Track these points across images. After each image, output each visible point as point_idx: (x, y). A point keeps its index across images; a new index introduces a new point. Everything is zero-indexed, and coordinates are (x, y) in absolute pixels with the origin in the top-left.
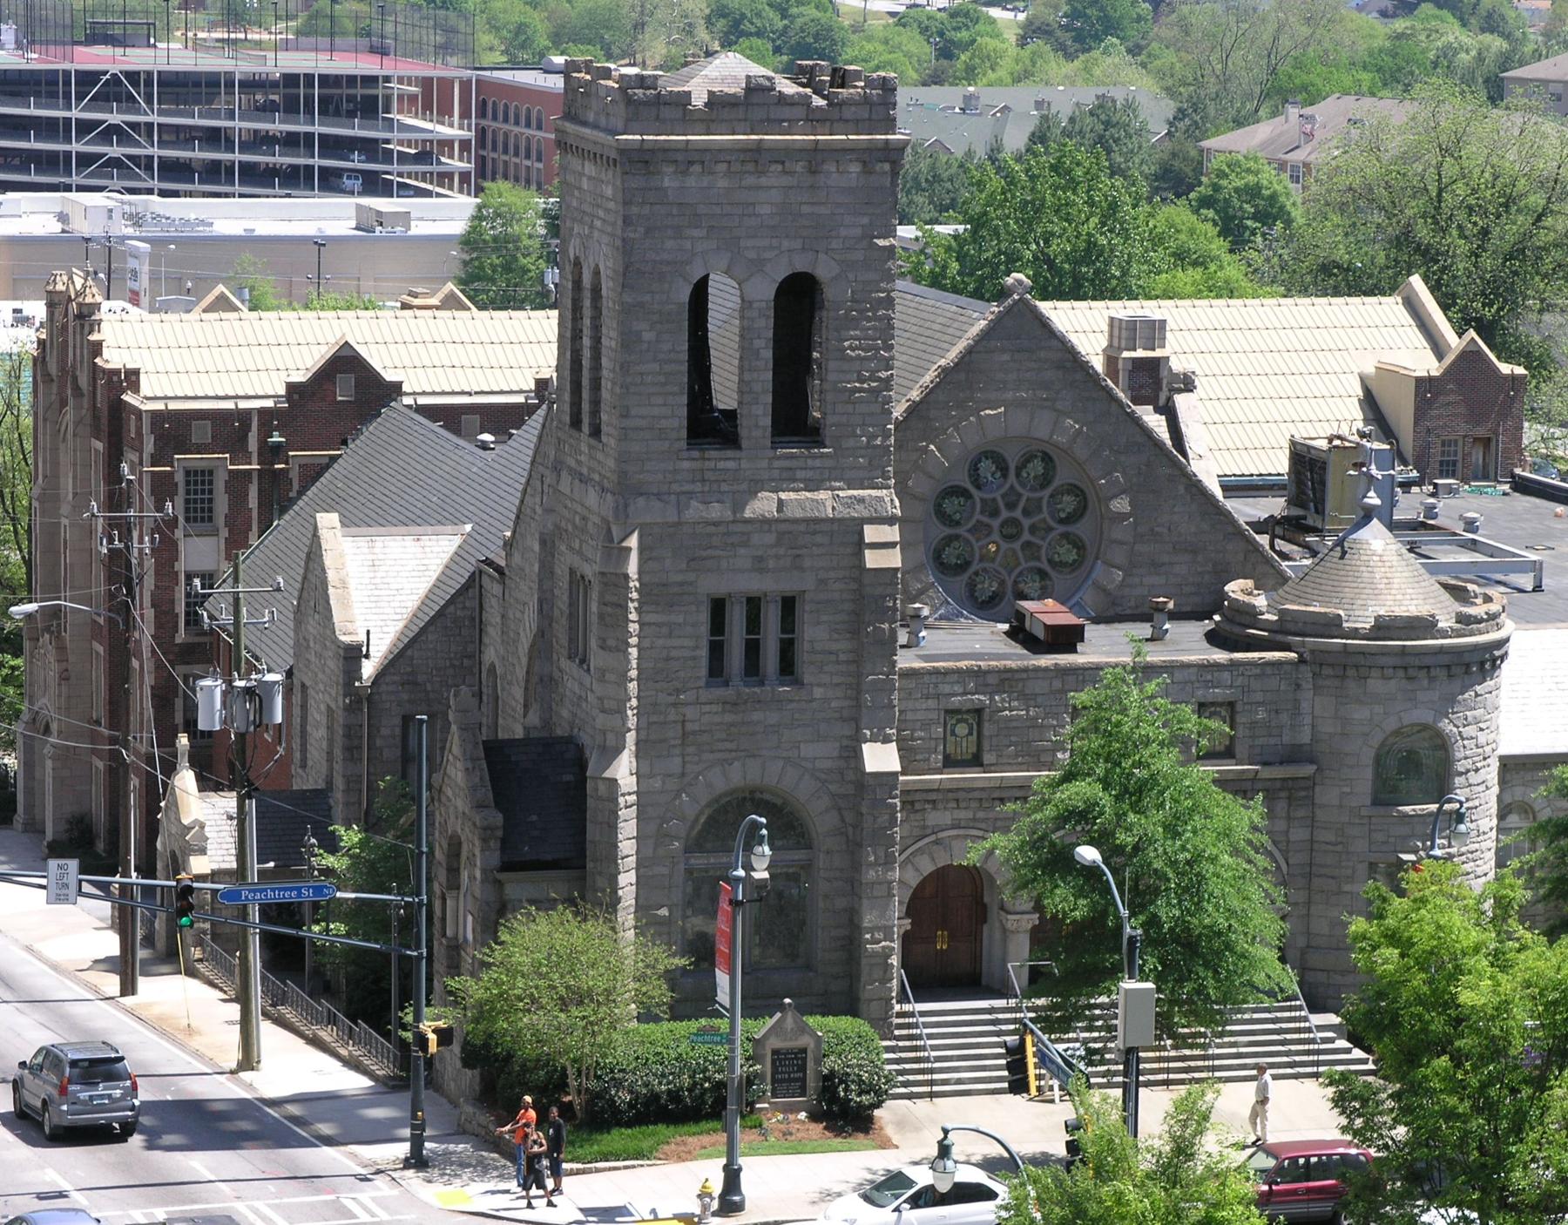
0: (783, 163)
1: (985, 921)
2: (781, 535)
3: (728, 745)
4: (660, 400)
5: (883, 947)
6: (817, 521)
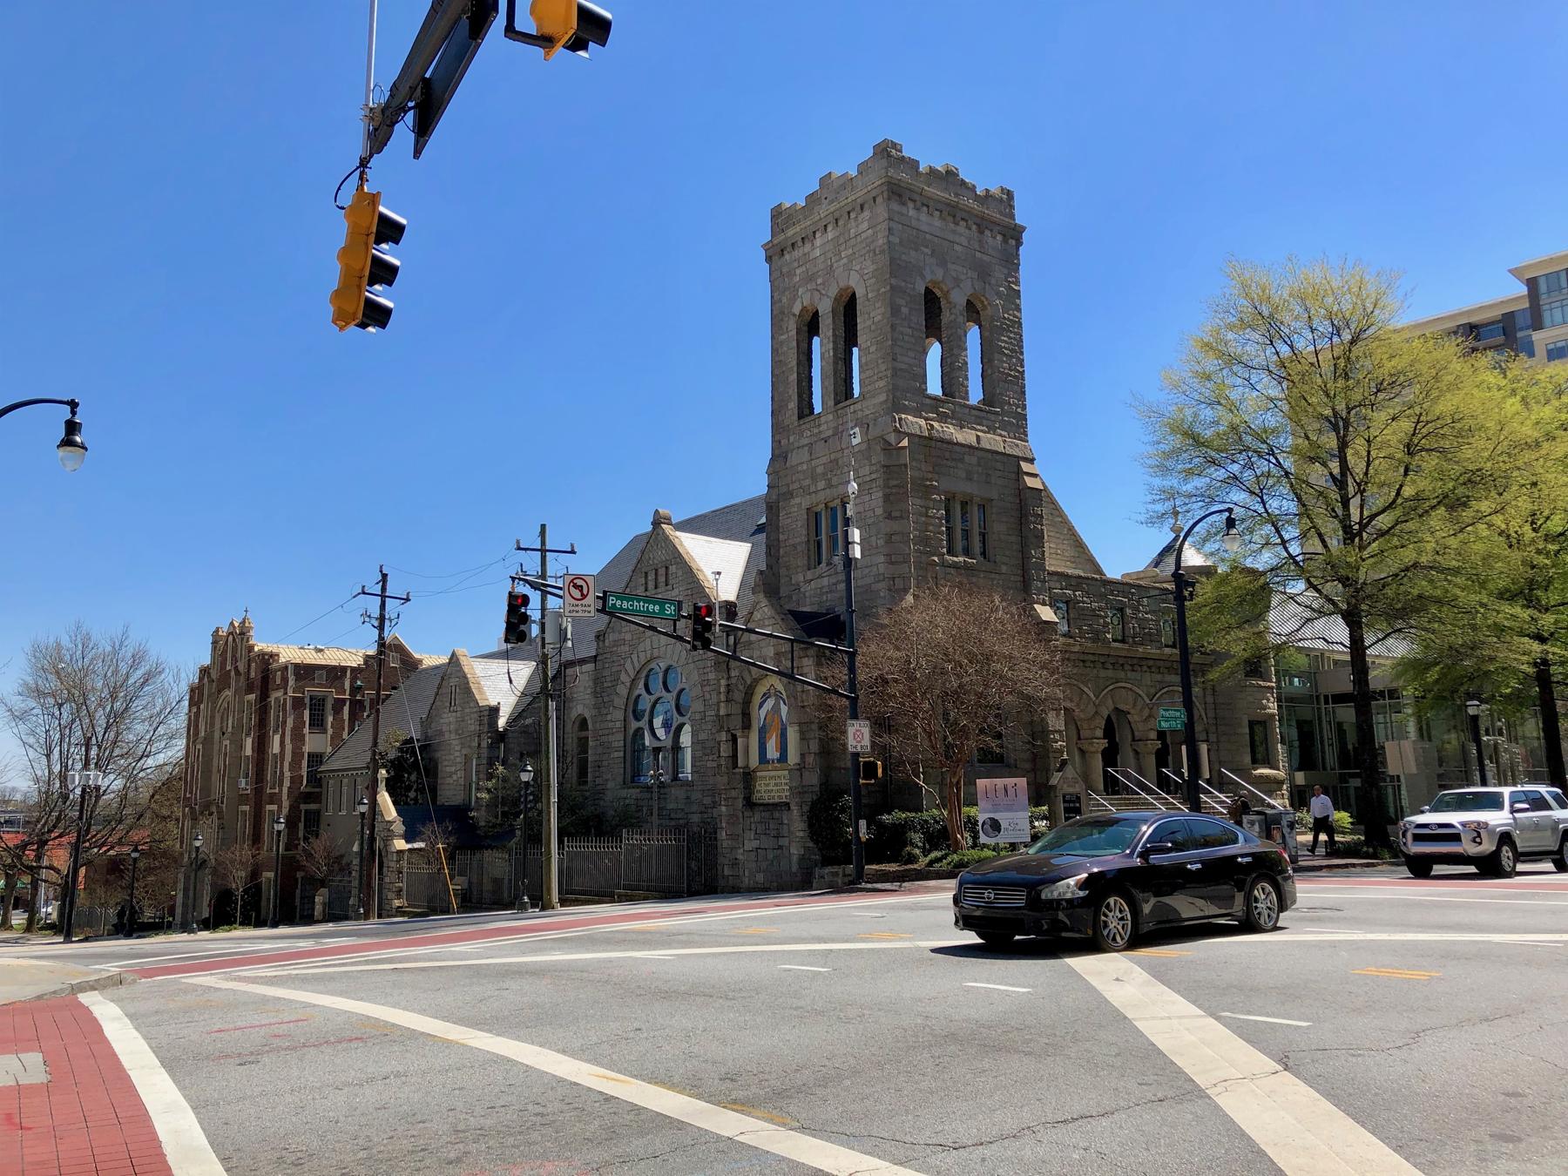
0: (967, 221)
5: (1061, 745)
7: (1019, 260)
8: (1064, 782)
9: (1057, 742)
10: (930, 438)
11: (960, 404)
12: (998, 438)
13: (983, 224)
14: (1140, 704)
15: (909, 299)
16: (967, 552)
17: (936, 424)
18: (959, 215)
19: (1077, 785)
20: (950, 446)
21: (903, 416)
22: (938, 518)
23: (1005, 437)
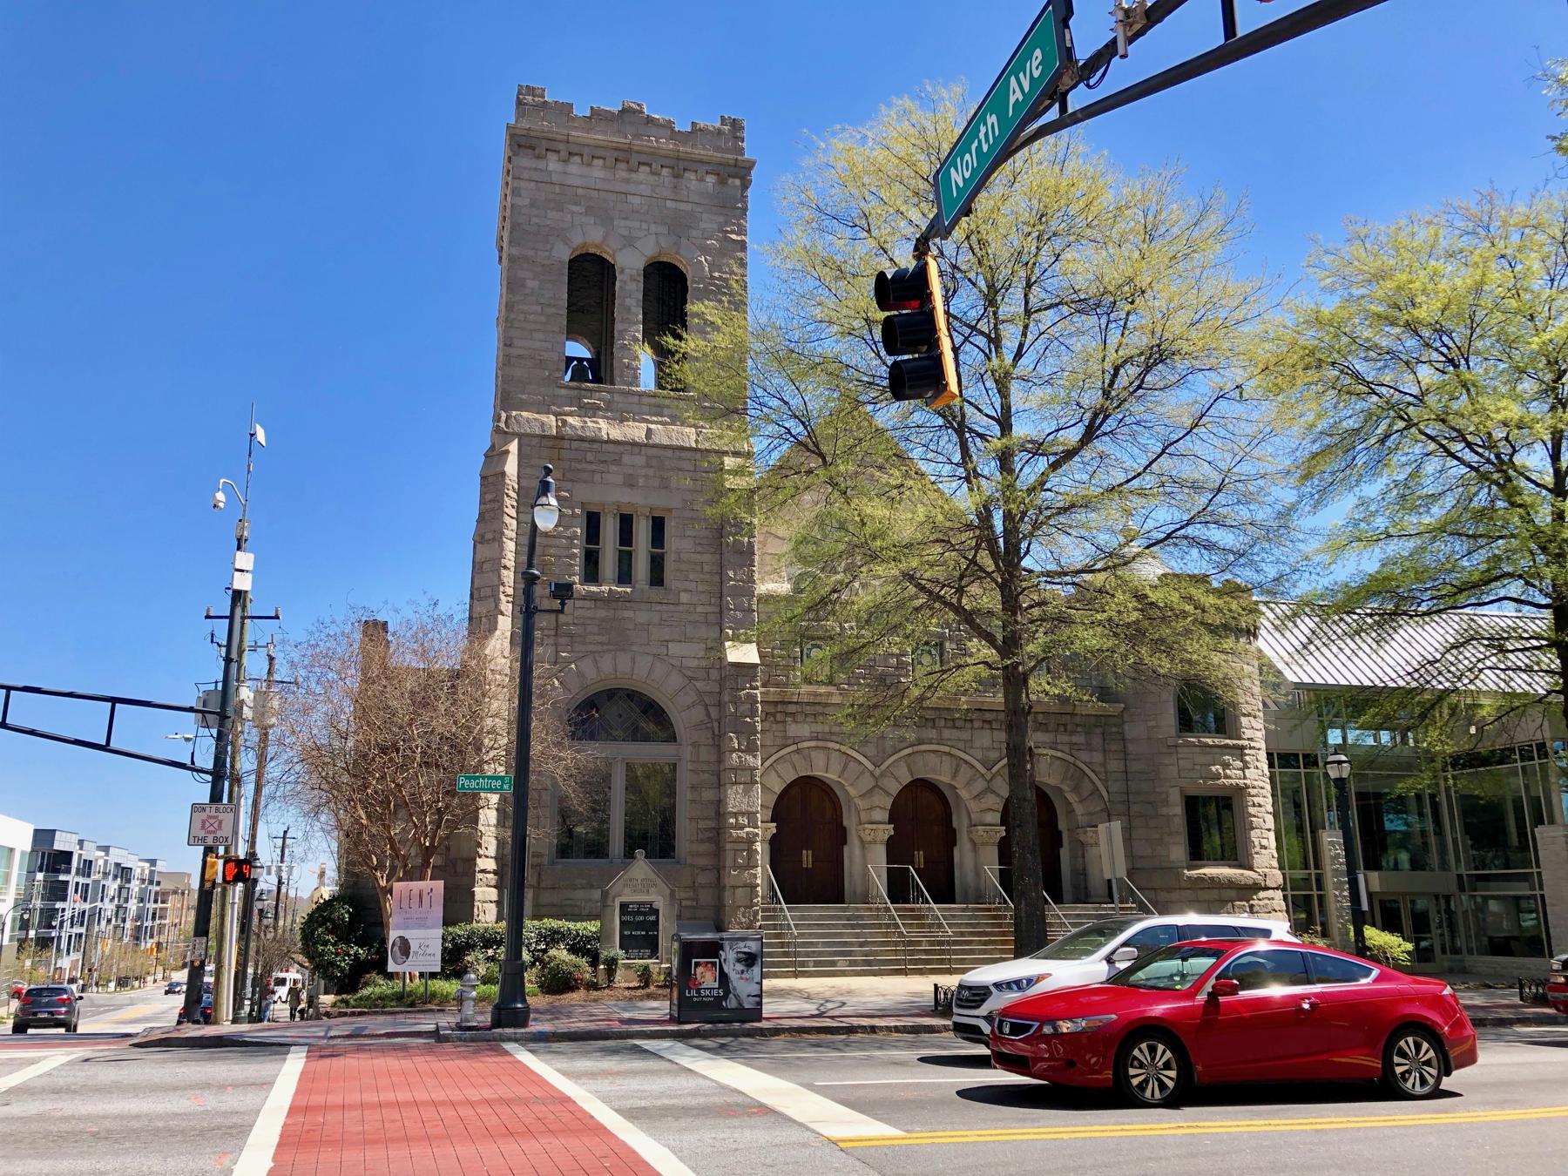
0: (650, 165)
1: (844, 842)
2: (649, 457)
3: (599, 638)
4: (541, 336)
5: (748, 833)
6: (682, 448)
7: (745, 203)
8: (625, 886)
9: (742, 828)
10: (560, 437)
11: (623, 393)
12: (687, 430)
13: (679, 166)
14: (965, 773)
15: (539, 269)
16: (624, 577)
17: (570, 420)
18: (635, 159)
19: (652, 890)
20: (595, 446)
21: (514, 413)
22: (567, 538)
23: (702, 427)
